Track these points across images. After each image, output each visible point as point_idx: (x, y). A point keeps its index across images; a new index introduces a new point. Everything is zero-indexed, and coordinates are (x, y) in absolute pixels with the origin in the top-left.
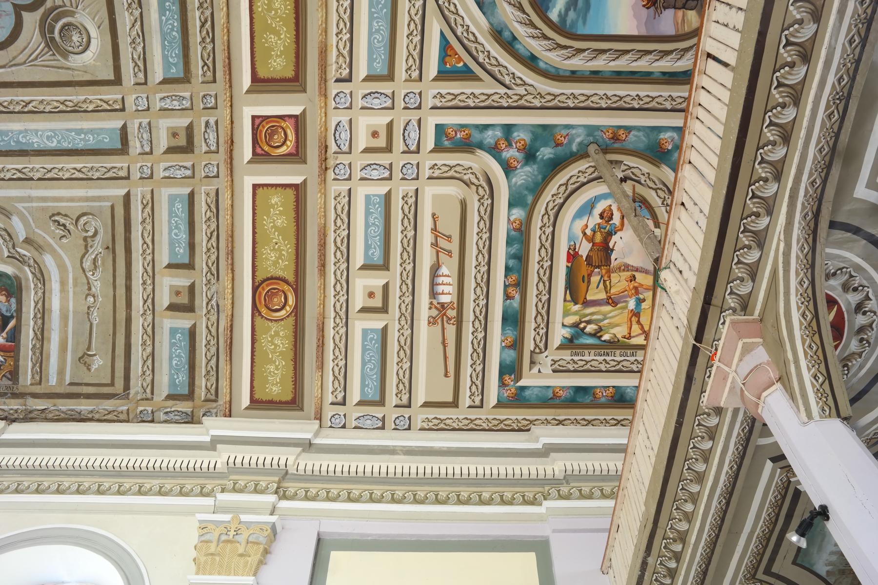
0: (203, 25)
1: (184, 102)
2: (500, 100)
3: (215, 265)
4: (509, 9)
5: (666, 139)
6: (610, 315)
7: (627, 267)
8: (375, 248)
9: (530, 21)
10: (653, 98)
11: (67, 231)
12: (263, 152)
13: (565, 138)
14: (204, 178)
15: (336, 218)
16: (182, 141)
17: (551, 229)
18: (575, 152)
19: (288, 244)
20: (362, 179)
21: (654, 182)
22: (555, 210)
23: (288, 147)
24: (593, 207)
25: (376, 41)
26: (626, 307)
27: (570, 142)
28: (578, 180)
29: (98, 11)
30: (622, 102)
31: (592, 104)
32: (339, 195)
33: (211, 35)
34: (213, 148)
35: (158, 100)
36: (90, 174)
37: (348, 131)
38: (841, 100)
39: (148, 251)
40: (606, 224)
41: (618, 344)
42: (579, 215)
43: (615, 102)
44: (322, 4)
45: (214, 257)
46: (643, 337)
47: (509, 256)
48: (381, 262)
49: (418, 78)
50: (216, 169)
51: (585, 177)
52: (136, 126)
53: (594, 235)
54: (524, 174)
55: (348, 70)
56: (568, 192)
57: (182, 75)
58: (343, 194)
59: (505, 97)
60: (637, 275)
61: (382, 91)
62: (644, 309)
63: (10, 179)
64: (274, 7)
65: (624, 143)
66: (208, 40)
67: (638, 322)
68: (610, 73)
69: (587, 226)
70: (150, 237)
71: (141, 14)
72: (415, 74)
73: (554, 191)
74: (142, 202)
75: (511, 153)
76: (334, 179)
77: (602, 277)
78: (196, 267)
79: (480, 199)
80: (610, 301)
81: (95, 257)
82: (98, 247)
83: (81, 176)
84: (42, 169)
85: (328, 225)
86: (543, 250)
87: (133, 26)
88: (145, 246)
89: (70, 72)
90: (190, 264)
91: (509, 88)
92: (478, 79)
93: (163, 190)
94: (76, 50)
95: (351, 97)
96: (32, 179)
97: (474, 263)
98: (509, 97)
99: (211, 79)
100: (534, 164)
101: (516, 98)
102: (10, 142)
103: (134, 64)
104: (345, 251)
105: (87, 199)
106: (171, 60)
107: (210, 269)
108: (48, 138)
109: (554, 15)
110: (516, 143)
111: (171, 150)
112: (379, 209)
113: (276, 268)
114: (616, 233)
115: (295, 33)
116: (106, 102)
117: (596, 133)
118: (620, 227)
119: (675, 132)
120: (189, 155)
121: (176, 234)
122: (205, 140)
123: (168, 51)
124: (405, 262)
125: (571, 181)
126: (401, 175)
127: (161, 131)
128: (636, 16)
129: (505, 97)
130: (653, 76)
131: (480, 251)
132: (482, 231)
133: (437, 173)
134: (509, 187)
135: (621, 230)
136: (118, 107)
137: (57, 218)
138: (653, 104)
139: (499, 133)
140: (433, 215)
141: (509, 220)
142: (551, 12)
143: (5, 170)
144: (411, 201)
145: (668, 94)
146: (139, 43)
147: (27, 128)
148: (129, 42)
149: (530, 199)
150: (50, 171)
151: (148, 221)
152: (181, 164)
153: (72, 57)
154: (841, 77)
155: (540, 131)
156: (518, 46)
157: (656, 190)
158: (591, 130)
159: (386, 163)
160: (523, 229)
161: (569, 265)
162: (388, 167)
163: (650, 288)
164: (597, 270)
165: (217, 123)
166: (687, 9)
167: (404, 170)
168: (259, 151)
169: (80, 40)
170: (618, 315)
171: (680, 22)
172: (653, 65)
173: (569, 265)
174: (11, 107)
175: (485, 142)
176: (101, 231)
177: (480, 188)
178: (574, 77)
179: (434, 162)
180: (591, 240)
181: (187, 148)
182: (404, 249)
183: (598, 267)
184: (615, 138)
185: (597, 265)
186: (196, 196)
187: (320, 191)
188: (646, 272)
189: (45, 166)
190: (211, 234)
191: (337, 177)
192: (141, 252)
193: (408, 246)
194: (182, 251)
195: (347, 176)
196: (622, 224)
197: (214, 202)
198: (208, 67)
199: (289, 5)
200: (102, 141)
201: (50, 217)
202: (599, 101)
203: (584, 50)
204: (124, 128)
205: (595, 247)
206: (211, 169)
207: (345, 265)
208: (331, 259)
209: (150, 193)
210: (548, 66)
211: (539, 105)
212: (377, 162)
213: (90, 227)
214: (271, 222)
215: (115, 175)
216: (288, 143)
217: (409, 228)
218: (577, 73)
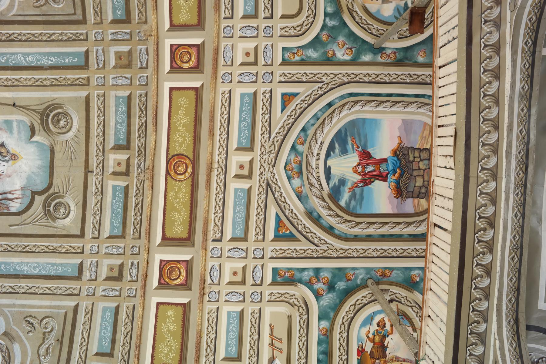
0: (136, 206)
1: (120, 250)
2: (312, 253)
3: (127, 355)
4: (316, 200)
8: (232, 346)
9: (329, 206)
10: (405, 250)
11: (33, 328)
12: (165, 283)
13: (352, 276)
14: (127, 297)
15: (208, 326)
16: (116, 274)
17: (346, 334)
19: (176, 342)
20: (226, 301)
21: (410, 302)
22: (348, 322)
23: (181, 280)
24: (372, 319)
25: (237, 217)
27: (356, 278)
28: (362, 302)
29: (78, 196)
30: (386, 253)
31: (368, 255)
32: (211, 311)
33: (140, 211)
34: (134, 279)
35: (104, 248)
36: (55, 291)
37: (219, 271)
38: (517, 249)
39: (85, 344)
42: (364, 324)
43: (382, 253)
44: (207, 196)
45: (127, 349)
47: (320, 353)
48: (236, 356)
49: (262, 240)
50: (135, 292)
52: (89, 263)
54: (328, 299)
55: (220, 234)
56: (356, 310)
57: (120, 234)
58: (213, 311)
59: (315, 251)
61: (240, 247)
63: (5, 293)
64: (179, 197)
65: (389, 278)
66: (138, 214)
68: (378, 236)
69: (369, 331)
70: (87, 334)
71: (102, 198)
72: (261, 238)
73: (347, 309)
74: (85, 311)
75: (319, 286)
76: (208, 301)
78: (115, 355)
79: (300, 315)
81: (49, 346)
82: (51, 339)
83: (49, 292)
84: (26, 287)
85: (203, 331)
86: (342, 348)
87: (96, 204)
88: (83, 340)
89: (55, 229)
90: (110, 353)
91: (317, 246)
92: (298, 240)
93: (100, 303)
94: (61, 217)
95: (221, 250)
96: (18, 293)
97: (297, 357)
98: (317, 251)
99: (138, 237)
100: (334, 292)
101: (321, 252)
102: (10, 270)
103: (93, 226)
104: (213, 348)
105: (51, 307)
106: (115, 225)
107: (123, 357)
108: (34, 268)
109: (342, 203)
110: (322, 279)
111: (108, 279)
112: (236, 321)
113: (167, 358)
114: (388, 336)
115: (190, 212)
116: (73, 248)
117: (371, 273)
119: (420, 270)
120: (119, 282)
121: (104, 333)
122: (130, 273)
123: (114, 220)
124: (252, 356)
125: (358, 303)
126: (250, 300)
127: (103, 267)
129: (315, 251)
130: (403, 237)
131: (300, 349)
132: (302, 335)
133: (273, 298)
134: (319, 307)
135: (392, 333)
136: (79, 251)
137: (28, 319)
138: (405, 254)
139: (311, 273)
140: (271, 325)
141: (319, 328)
142: (341, 201)
143: (3, 286)
144: (257, 316)
145: (414, 247)
146: (98, 214)
147: (22, 261)
148: (92, 213)
149: (332, 314)
150: (31, 288)
151: (87, 323)
152: (113, 288)
153: (58, 221)
154: (515, 235)
155: (337, 272)
156: (322, 221)
157: (411, 307)
158: (368, 270)
159: (241, 291)
160: (328, 334)
161: (359, 358)
162: (242, 294)
164: (377, 361)
165: (138, 263)
167: (253, 296)
168: (162, 281)
169: (64, 211)
171: (416, 205)
172: (403, 230)
173: (359, 358)
174: (16, 249)
175: (303, 279)
176: (56, 329)
177: (300, 308)
178: (356, 239)
179: (271, 291)
180: (372, 341)
181: (118, 278)
182: (251, 347)
183: (378, 359)
184: (384, 275)
186: (120, 308)
187: (199, 308)
189: (28, 285)
190: (127, 333)
191: (211, 300)
192: (79, 344)
193: (254, 345)
194: (107, 344)
195: (216, 299)
196: (392, 330)
197: (131, 313)
198: (137, 230)
199: (187, 196)
200: (66, 271)
201: (24, 318)
202: (372, 253)
203: (361, 223)
204: (81, 265)
206: (132, 292)
207: (213, 357)
208: (203, 353)
209: (91, 305)
210: (340, 233)
211: (336, 256)
212: (236, 291)
213: (49, 325)
214: (166, 328)
215: (71, 292)
216: (181, 277)
217: (255, 334)
218: (358, 236)
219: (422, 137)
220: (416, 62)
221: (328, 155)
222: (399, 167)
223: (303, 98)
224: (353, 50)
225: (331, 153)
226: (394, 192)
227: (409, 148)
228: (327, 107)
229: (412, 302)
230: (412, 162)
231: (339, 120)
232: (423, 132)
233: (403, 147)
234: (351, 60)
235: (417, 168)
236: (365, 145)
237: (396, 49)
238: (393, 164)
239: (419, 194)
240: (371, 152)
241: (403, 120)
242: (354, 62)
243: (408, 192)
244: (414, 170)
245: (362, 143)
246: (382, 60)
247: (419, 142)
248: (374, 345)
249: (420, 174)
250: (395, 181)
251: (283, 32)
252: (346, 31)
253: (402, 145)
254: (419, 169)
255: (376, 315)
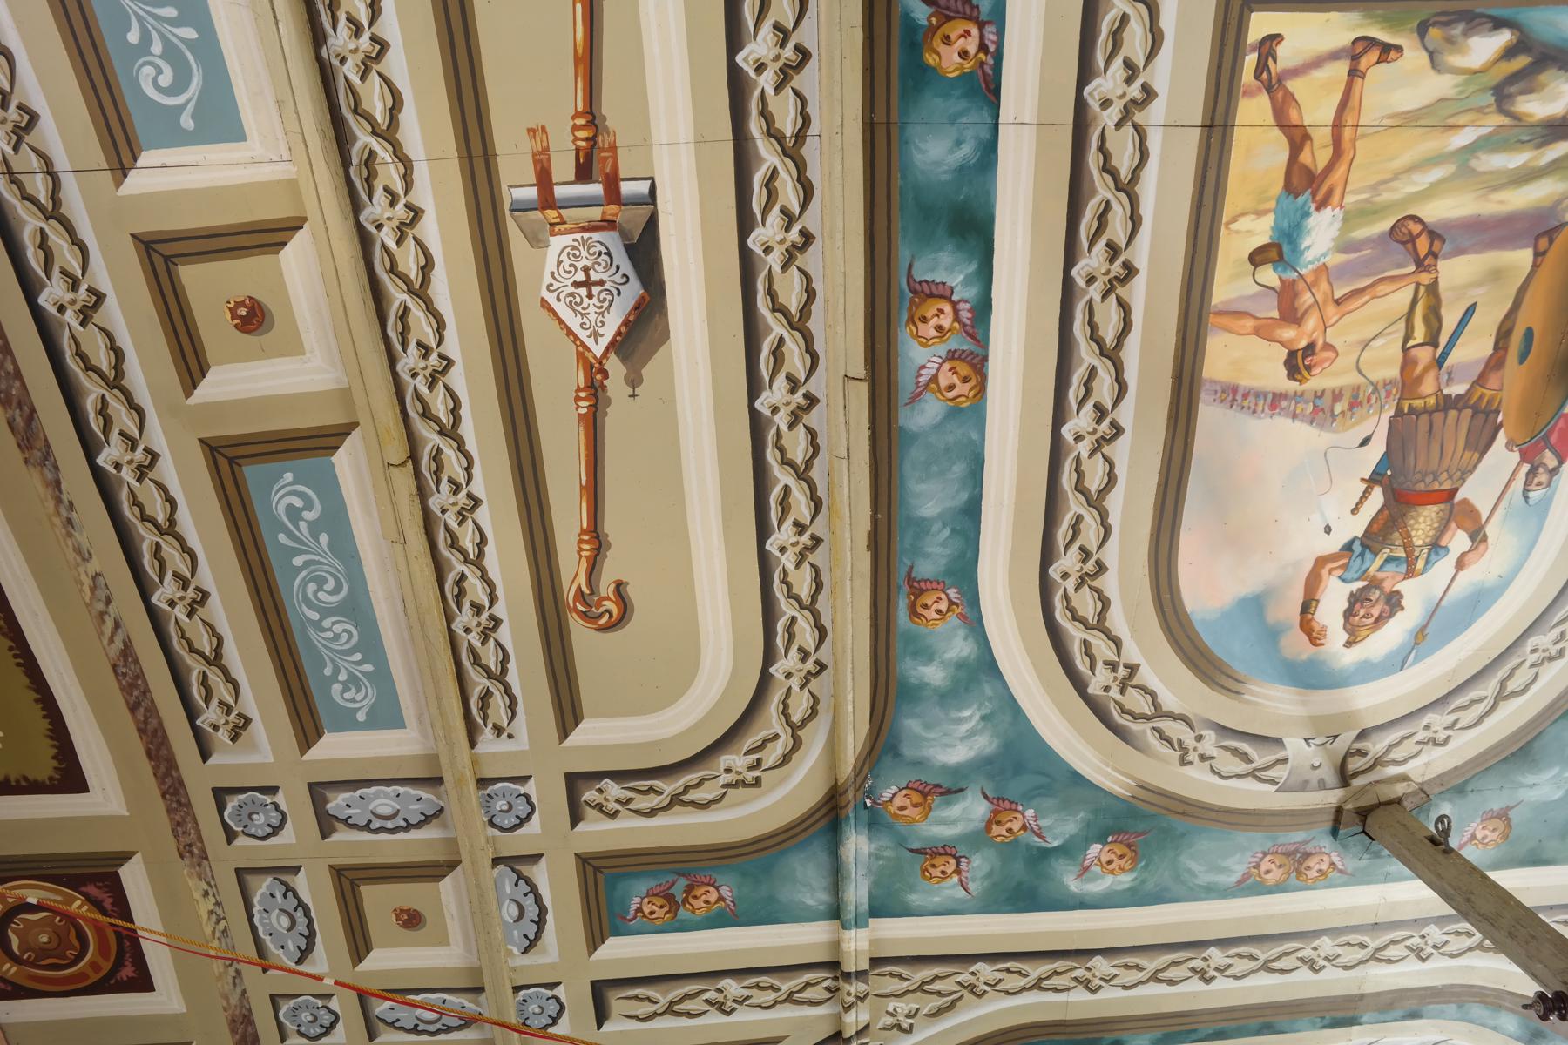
5: (1112, 872)
6: (1436, 174)
7: (1322, 410)
10: (1154, 978)
13: (1473, 837)
18: (1443, 800)
21: (1163, 737)
26: (1350, 219)
28: (1453, 717)
30: (1263, 957)
40: (1381, 575)
41: (1425, 12)
42: (1479, 601)
46: (1286, 55)
51: (1427, 727)
53: (1442, 530)
56: (1502, 672)
60: (1277, 379)
62: (1260, 213)
65: (1268, 845)
67: (1298, 138)
69: (1460, 564)
77: (1439, 362)
80: (1423, 245)
114: (1348, 547)
118: (1325, 572)
119: (1074, 896)
135: (1321, 562)
157: (1159, 712)
163: (1223, 320)
164: (1458, 389)
170: (1396, 176)
183: (1448, 404)
185: (1453, 413)
188: (1232, 395)
196: (1313, 584)
202: (1339, 950)
205: (1447, 486)
229: (1153, 740)
248: (1454, 492)
255: (1390, 657)
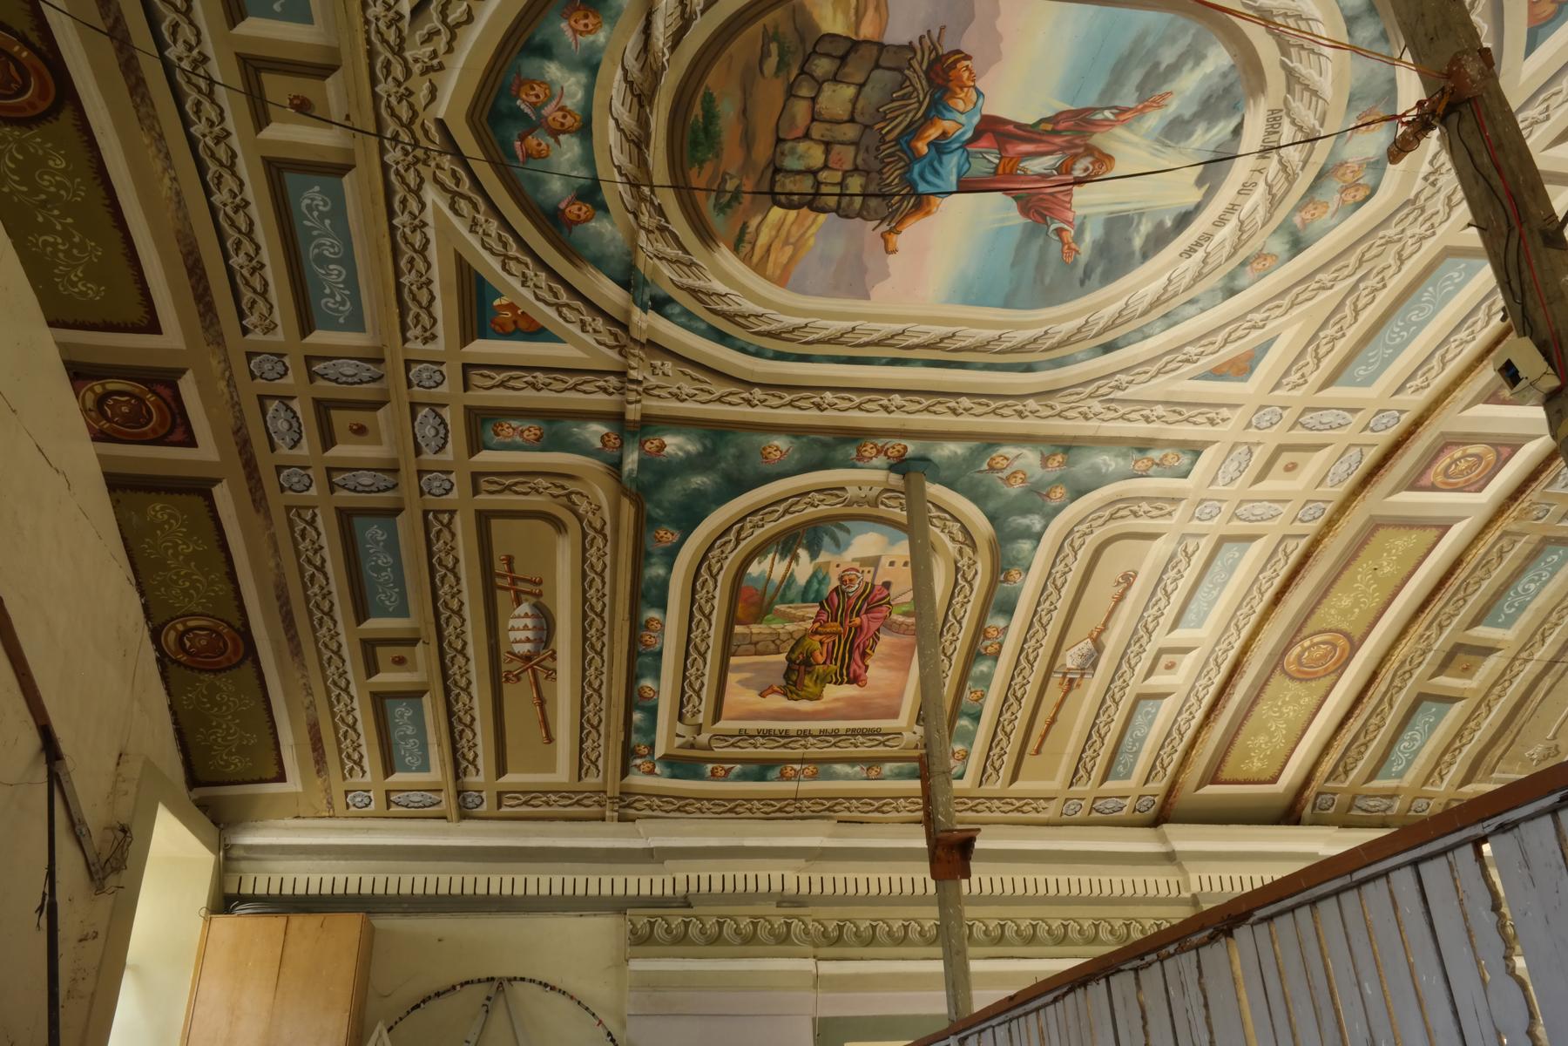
128: (994, 39)
166: (847, 38)
171: (870, 13)
219: (798, 245)
220: (796, 437)
221: (1184, 219)
222: (916, 157)
223: (1188, 367)
224: (985, 467)
225: (1169, 223)
226: (966, 75)
227: (859, 215)
228: (1120, 344)
230: (856, 169)
231: (1096, 308)
232: (791, 259)
233: (883, 220)
234: (1000, 445)
235: (837, 148)
236: (1029, 235)
237: (854, 467)
238: (937, 173)
239: (847, 54)
240: (1017, 213)
241: (867, 297)
242: (991, 441)
243: (899, 70)
244: (852, 143)
245: (1040, 241)
246: (904, 442)
247: (813, 230)
249: (828, 126)
250: (948, 115)
251: (1169, 508)
252: (991, 505)
253: (884, 227)
254: (828, 145)
